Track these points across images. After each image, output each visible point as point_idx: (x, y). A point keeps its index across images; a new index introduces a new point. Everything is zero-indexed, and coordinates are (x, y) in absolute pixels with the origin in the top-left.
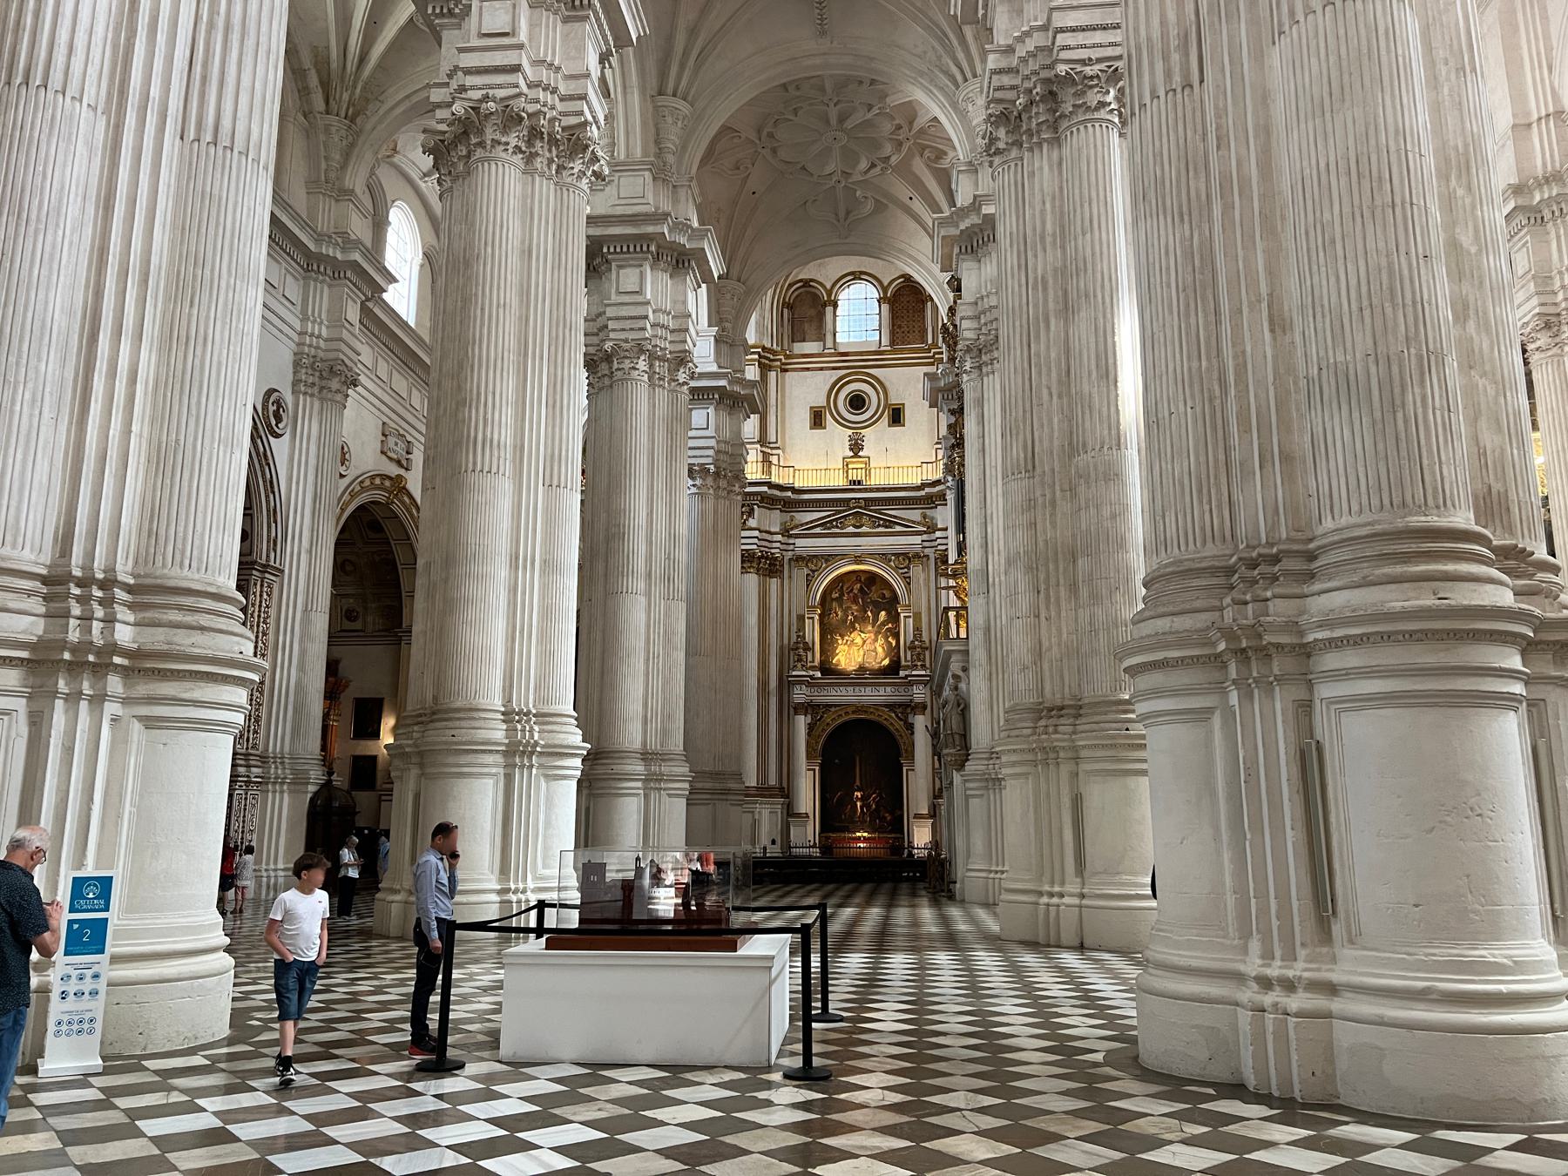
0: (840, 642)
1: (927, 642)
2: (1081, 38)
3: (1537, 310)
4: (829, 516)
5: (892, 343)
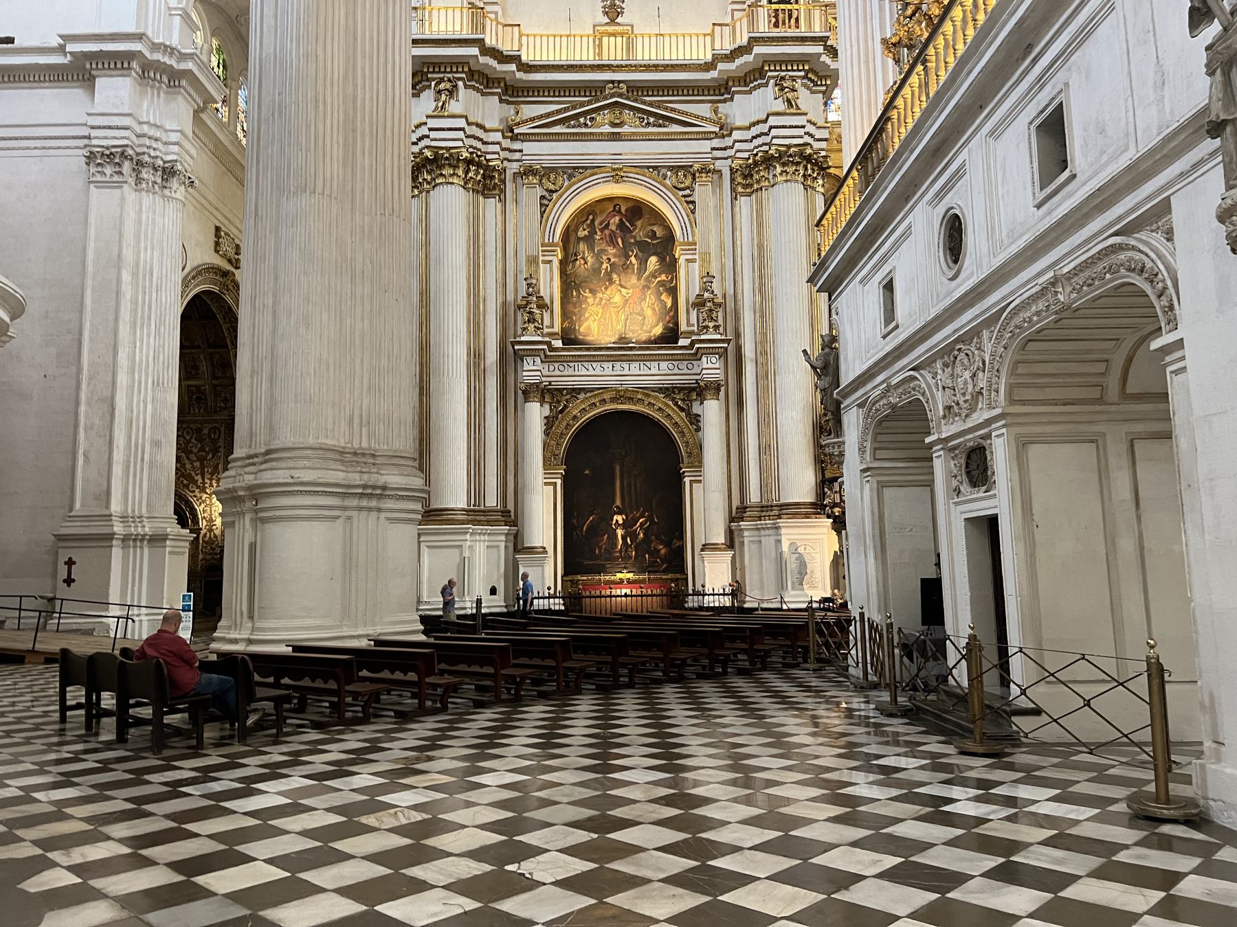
0: (590, 301)
1: (720, 296)
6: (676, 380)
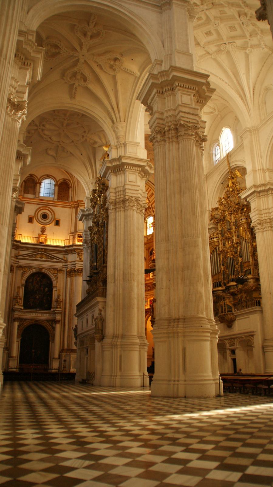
1: (62, 299)
2: (186, 115)
3: (258, 219)
4: (32, 253)
5: (58, 199)
6: (49, 318)
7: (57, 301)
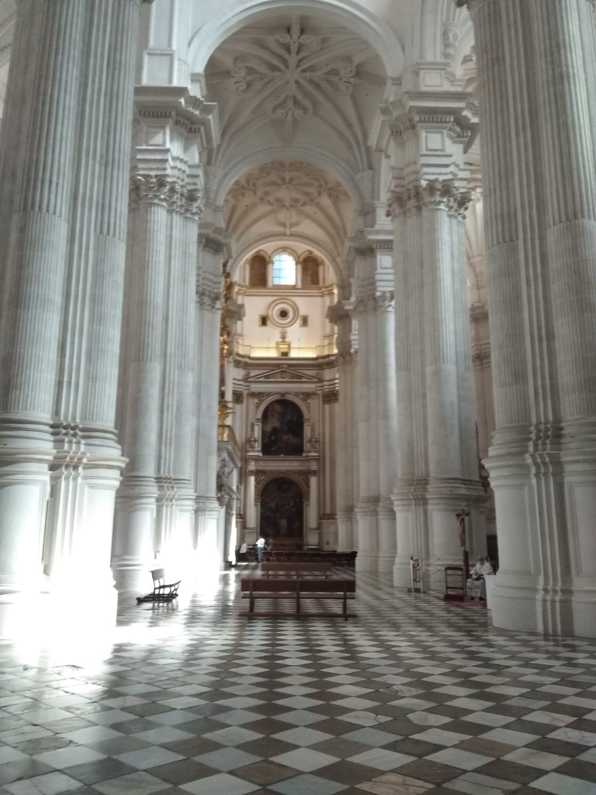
7: (310, 441)
